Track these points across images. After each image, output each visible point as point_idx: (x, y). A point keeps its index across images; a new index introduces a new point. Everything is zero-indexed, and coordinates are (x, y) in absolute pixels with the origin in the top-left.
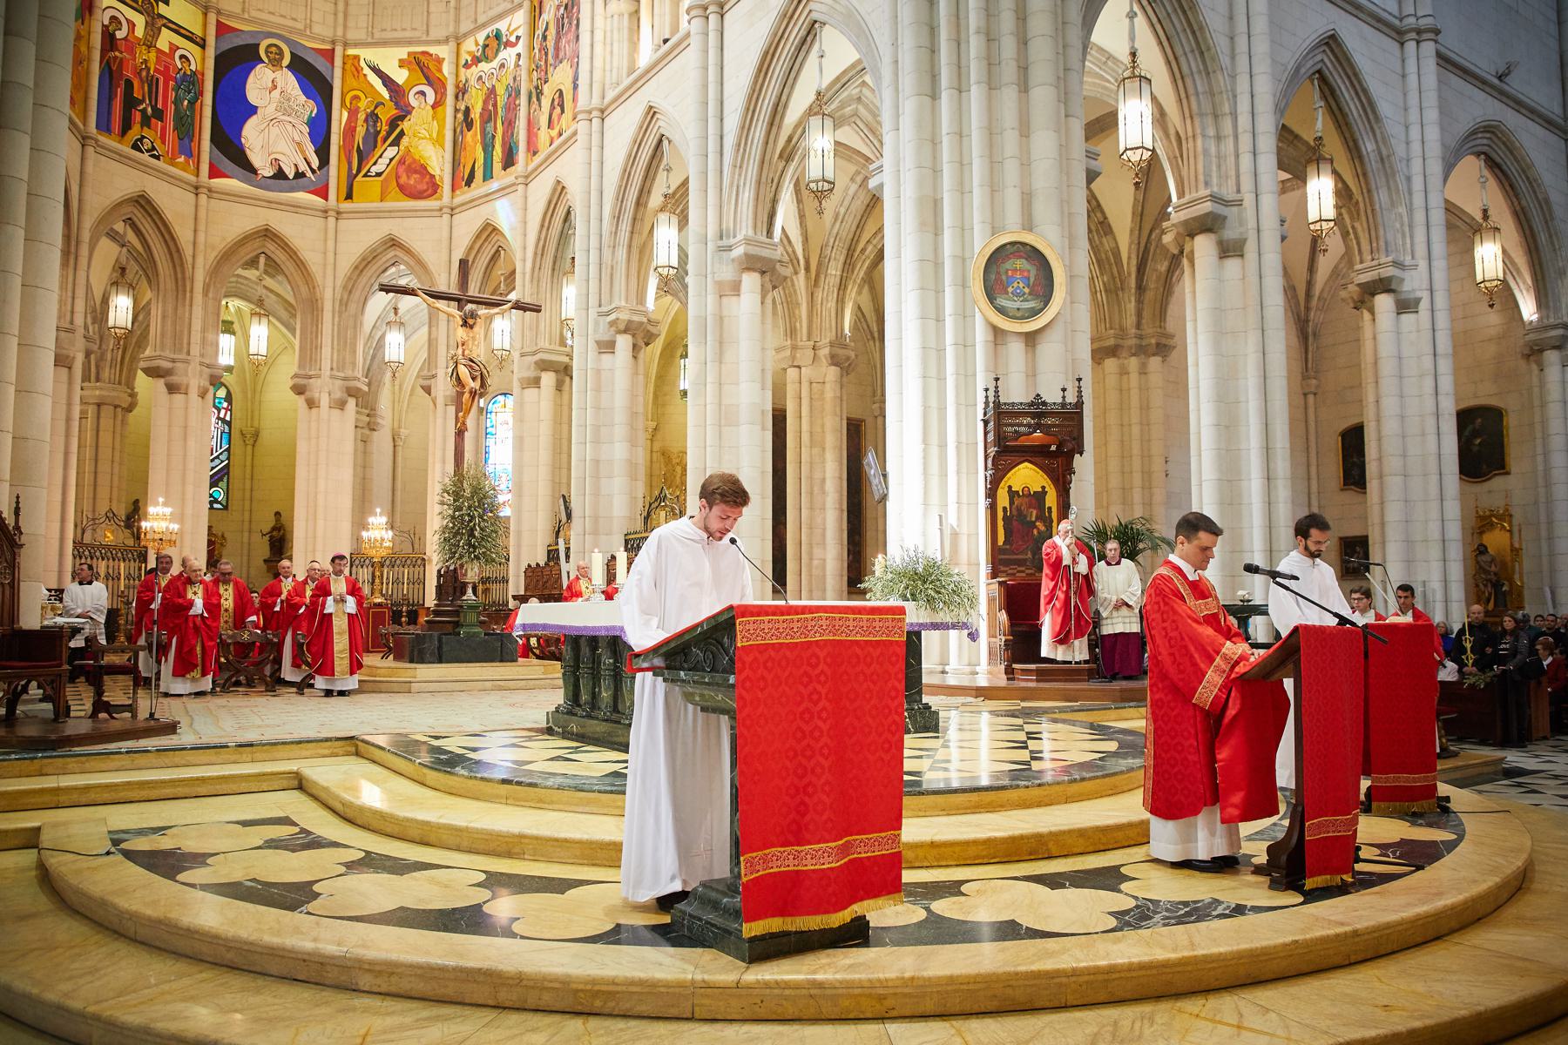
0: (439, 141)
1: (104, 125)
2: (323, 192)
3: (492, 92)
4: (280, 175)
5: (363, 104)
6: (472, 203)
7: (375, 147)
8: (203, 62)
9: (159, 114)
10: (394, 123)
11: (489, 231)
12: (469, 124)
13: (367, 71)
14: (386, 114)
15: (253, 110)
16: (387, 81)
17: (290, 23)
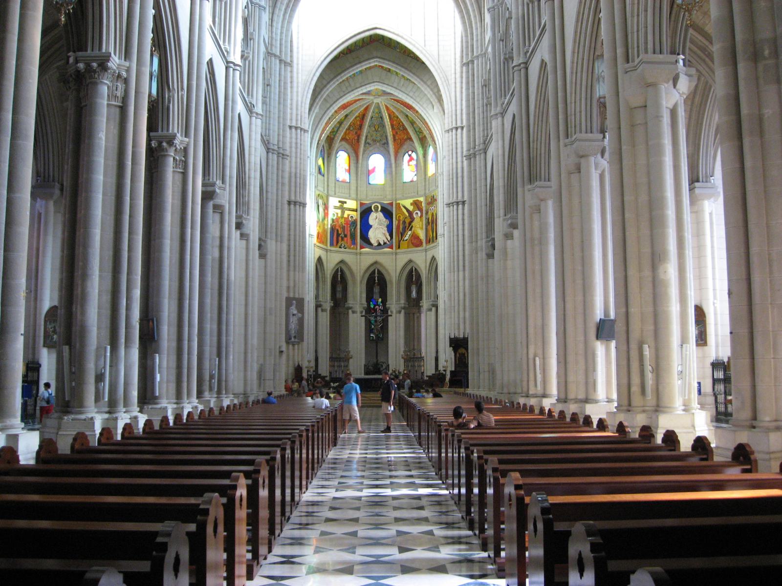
0: (422, 228)
1: (332, 245)
2: (392, 248)
3: (433, 214)
4: (379, 244)
5: (401, 218)
6: (430, 249)
7: (405, 231)
8: (356, 216)
9: (345, 236)
10: (410, 223)
11: (433, 259)
12: (429, 223)
13: (402, 207)
14: (408, 221)
15: (371, 226)
16: (408, 210)
17: (380, 197)
